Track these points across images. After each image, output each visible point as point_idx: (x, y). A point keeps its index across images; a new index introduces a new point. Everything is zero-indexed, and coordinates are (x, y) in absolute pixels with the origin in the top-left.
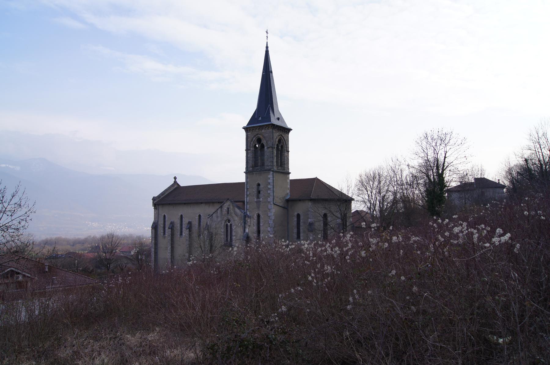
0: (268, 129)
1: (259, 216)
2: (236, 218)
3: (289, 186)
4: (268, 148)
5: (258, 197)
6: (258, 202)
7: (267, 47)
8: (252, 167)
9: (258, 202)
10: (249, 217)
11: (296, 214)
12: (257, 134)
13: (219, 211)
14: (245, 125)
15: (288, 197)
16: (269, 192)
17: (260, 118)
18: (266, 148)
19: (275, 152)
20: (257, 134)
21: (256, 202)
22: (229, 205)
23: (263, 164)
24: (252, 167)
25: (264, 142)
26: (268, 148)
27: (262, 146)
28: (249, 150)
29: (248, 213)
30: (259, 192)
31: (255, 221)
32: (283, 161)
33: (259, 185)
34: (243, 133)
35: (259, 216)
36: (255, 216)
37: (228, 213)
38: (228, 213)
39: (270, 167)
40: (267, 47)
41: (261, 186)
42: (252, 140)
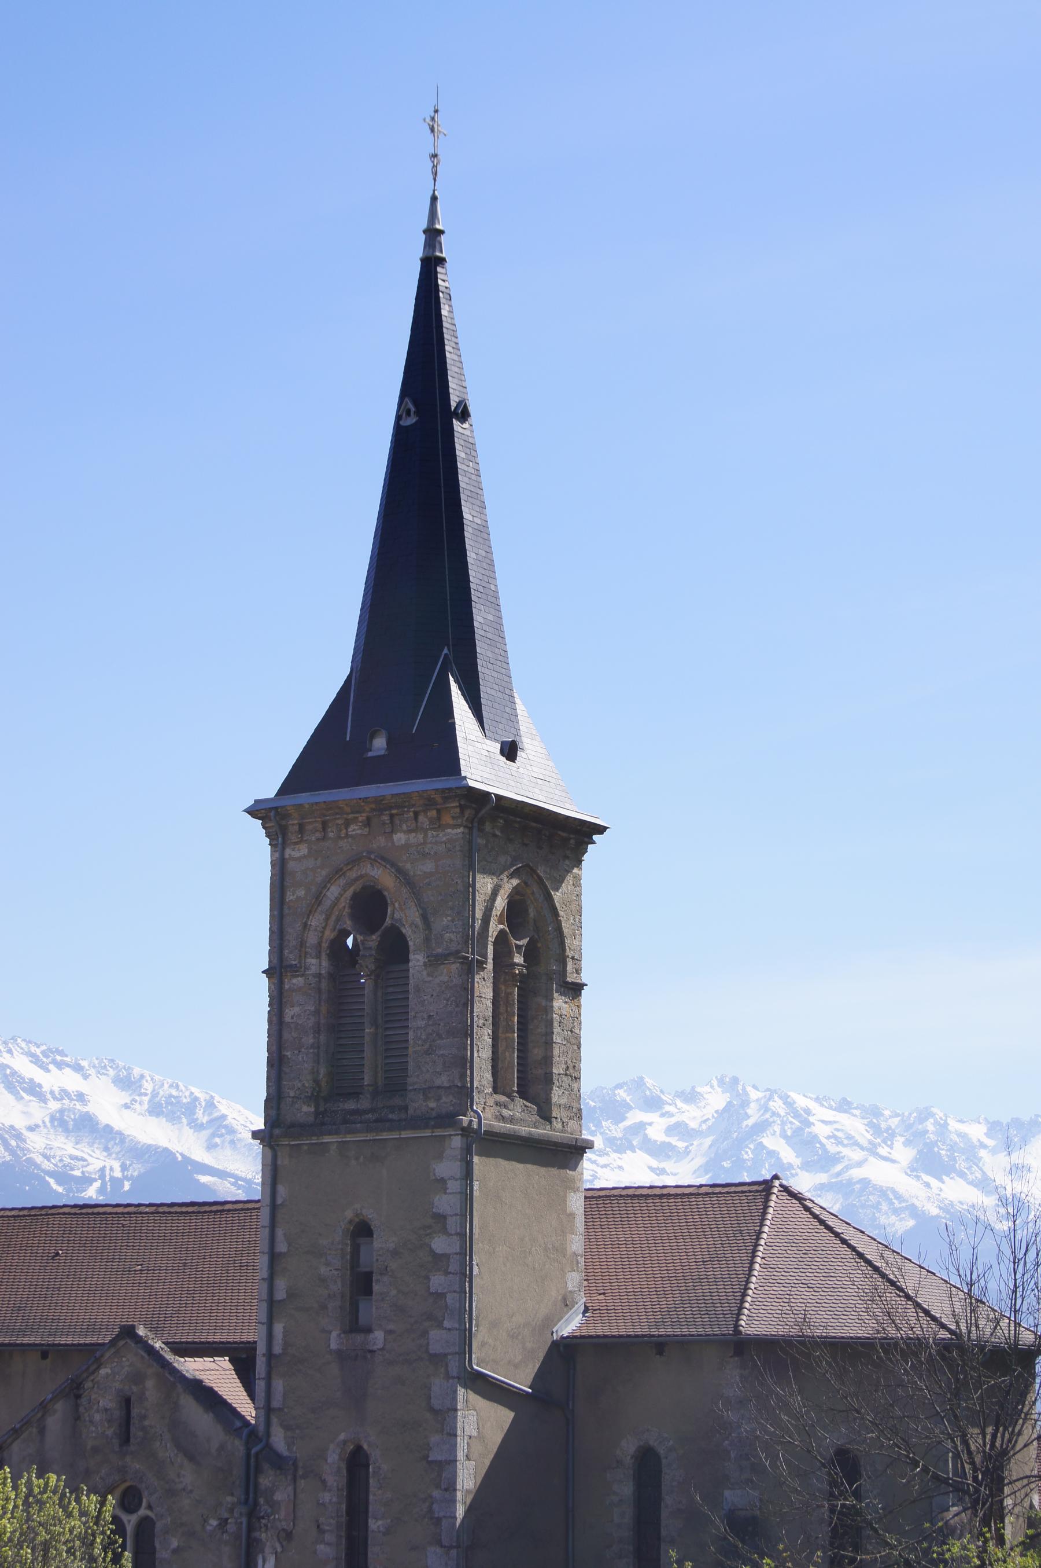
0: (438, 824)
1: (357, 1463)
2: (188, 1476)
3: (576, 1243)
4: (435, 961)
5: (355, 1326)
6: (355, 1360)
7: (433, 235)
8: (315, 1098)
9: (355, 1360)
10: (279, 1462)
11: (628, 1447)
12: (355, 861)
13: (55, 1422)
14: (269, 789)
15: (571, 1325)
16: (438, 1282)
17: (380, 744)
18: (417, 960)
19: (484, 988)
20: (355, 861)
21: (340, 1355)
22: (137, 1378)
23: (395, 1084)
24: (315, 1098)
25: (405, 914)
26: (435, 961)
27: (395, 950)
28: (295, 970)
29: (279, 1440)
30: (362, 1284)
31: (329, 1497)
32: (537, 1053)
33: (362, 1230)
34: (255, 846)
35: (357, 1463)
36: (333, 1456)
37: (125, 1438)
38: (125, 1438)
39: (447, 1102)
40: (433, 235)
41: (382, 1242)
42: (318, 899)
